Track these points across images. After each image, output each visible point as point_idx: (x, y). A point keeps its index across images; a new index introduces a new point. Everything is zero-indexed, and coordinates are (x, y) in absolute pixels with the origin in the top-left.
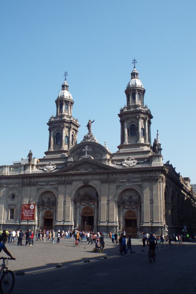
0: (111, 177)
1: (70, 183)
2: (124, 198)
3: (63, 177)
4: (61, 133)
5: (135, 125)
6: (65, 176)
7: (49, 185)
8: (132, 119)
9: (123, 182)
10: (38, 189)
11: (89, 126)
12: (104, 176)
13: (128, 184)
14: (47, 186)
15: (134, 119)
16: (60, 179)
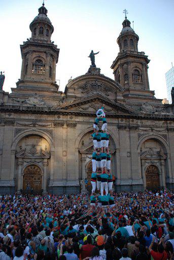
0: (131, 122)
1: (74, 125)
2: (144, 150)
3: (61, 116)
4: (44, 62)
5: (138, 71)
6: (64, 114)
7: (36, 126)
8: (136, 64)
9: (145, 130)
10: (18, 131)
11: (92, 56)
12: (122, 121)
13: (152, 133)
14: (34, 126)
15: (138, 64)
16: (57, 119)
